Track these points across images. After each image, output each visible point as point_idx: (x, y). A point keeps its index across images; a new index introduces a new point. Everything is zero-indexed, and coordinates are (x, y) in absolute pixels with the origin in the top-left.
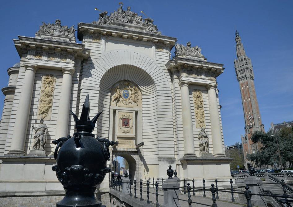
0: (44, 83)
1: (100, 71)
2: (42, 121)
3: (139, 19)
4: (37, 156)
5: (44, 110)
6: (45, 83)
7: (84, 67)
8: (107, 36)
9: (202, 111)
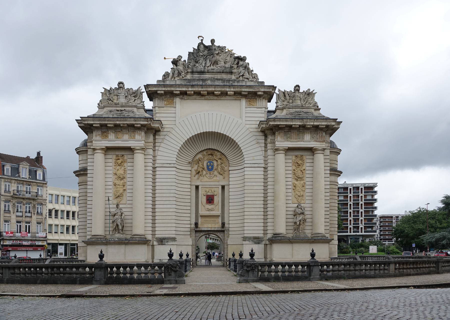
0: (115, 165)
1: (176, 143)
2: (117, 206)
3: (228, 55)
4: (117, 240)
5: (118, 194)
6: (116, 165)
7: (157, 141)
8: (181, 96)
9: (302, 182)
